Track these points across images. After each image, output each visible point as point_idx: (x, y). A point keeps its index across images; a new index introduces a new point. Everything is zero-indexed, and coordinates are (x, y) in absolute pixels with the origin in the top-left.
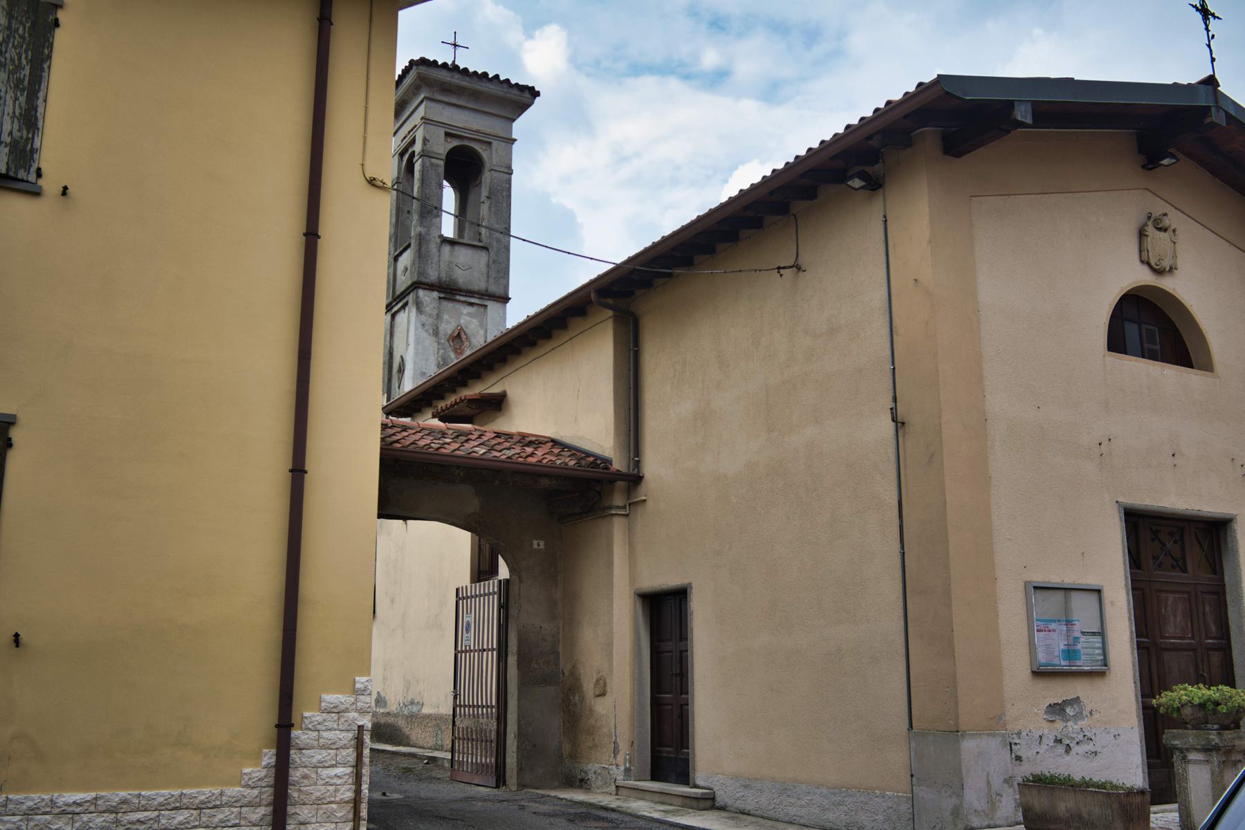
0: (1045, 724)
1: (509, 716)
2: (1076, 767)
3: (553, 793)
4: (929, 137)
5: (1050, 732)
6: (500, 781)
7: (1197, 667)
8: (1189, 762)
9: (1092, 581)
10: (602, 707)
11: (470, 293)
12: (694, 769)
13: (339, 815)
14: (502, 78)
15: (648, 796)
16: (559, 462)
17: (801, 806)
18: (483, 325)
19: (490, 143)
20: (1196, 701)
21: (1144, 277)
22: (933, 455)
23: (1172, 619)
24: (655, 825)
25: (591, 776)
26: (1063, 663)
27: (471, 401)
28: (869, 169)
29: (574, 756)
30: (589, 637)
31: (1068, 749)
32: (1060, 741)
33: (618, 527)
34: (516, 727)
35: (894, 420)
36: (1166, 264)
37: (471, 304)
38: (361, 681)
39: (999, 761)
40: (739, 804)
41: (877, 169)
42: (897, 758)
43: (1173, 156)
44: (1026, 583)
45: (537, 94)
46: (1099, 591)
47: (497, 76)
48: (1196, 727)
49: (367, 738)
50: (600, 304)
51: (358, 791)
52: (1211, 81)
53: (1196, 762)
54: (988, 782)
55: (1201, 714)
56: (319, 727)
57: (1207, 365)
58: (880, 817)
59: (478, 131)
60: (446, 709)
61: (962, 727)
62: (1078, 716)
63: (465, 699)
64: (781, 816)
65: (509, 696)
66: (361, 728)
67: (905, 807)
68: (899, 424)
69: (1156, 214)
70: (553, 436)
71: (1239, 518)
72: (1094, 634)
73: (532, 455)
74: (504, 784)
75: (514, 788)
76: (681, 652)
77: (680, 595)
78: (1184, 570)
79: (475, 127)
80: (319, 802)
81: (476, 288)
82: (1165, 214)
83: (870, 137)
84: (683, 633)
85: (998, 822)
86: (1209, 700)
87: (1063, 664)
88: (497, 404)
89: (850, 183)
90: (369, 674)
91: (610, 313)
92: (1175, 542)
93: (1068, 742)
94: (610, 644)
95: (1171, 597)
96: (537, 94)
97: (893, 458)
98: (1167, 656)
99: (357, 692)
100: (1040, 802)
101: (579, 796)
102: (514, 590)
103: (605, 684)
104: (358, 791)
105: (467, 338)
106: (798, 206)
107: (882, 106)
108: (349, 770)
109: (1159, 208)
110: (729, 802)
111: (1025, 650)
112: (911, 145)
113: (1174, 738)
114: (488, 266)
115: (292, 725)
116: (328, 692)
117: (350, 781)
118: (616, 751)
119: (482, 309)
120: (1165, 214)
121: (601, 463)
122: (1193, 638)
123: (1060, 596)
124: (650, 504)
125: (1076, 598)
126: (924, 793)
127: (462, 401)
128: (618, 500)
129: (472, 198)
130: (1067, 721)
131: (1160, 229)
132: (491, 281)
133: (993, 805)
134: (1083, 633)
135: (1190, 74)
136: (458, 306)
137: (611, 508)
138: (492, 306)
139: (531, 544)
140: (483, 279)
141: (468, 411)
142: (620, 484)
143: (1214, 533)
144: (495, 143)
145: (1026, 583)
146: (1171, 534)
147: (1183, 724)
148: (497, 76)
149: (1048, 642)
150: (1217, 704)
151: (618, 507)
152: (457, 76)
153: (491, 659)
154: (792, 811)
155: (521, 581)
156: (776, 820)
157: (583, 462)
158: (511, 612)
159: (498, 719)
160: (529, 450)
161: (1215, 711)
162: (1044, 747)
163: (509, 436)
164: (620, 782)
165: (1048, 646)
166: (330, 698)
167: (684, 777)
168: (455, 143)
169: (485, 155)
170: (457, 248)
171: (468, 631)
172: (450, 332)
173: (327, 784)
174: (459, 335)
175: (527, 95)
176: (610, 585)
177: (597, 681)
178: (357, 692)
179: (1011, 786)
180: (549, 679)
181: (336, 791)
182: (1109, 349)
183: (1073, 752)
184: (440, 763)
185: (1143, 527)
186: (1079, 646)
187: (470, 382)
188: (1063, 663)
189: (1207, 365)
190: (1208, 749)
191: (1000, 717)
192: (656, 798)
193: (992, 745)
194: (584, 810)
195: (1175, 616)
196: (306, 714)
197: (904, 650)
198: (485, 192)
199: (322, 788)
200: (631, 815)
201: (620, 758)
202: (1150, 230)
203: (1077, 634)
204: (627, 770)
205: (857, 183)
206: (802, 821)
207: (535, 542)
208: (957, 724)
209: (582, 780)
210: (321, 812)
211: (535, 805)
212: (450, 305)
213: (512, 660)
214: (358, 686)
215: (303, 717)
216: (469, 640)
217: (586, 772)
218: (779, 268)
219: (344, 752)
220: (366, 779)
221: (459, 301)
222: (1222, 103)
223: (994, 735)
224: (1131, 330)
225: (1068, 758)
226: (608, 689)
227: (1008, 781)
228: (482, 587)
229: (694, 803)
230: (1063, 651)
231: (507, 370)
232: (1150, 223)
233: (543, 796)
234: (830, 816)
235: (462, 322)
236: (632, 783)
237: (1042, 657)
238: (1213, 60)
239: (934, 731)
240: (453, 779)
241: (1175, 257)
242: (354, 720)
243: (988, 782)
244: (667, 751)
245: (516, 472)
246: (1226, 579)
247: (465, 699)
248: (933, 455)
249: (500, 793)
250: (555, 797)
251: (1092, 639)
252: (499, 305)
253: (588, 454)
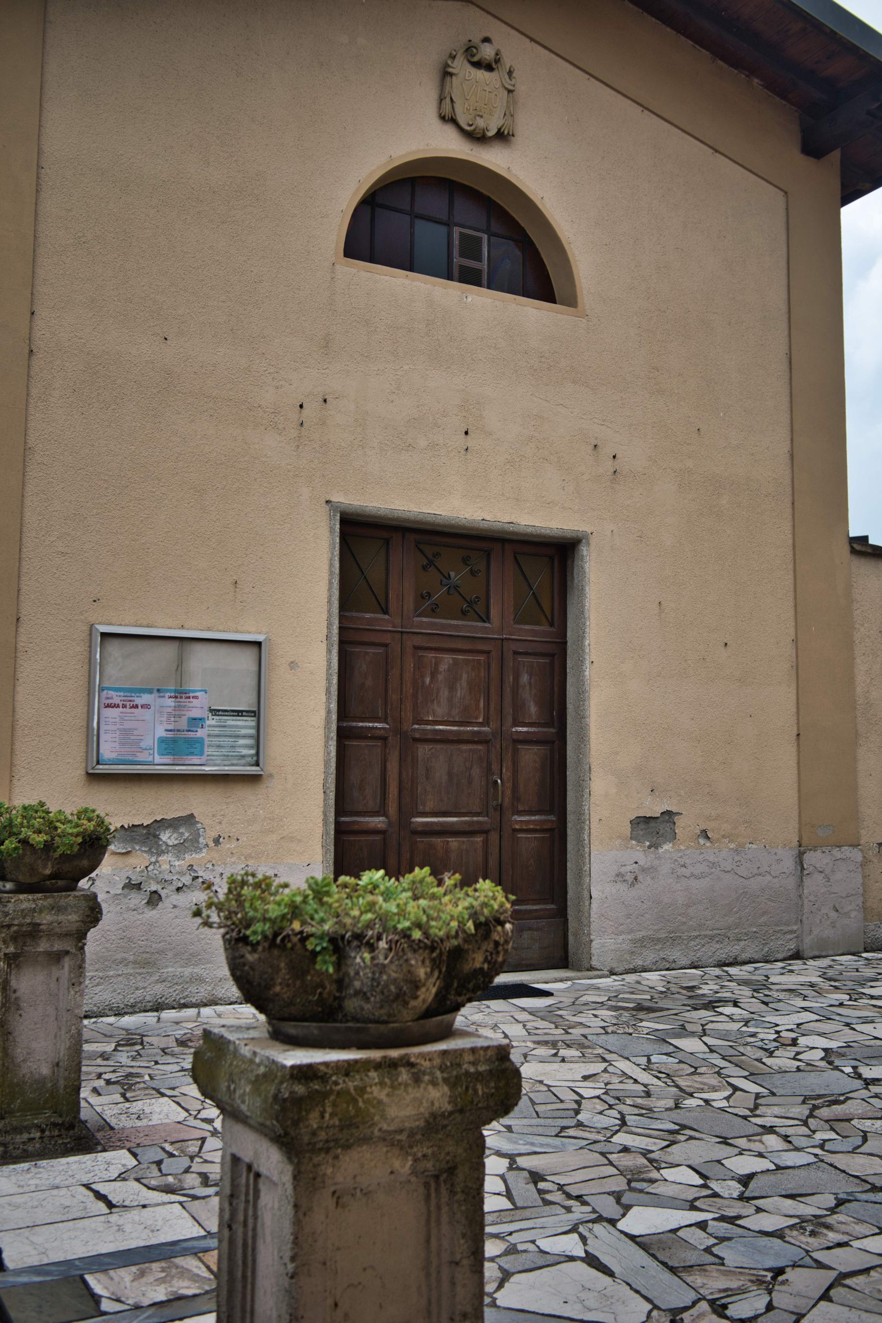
7: (489, 771)
21: (449, 145)
23: (444, 693)
26: (158, 759)
32: (138, 887)
46: (259, 644)
71: (593, 541)
78: (486, 618)
87: (160, 763)
92: (473, 573)
95: (447, 659)
130: (160, 853)
131: (477, 65)
134: (214, 712)
149: (127, 725)
182: (347, 255)
183: (166, 904)
188: (158, 759)
195: (452, 688)
225: (151, 914)
230: (162, 740)
241: (509, 114)
251: (240, 722)
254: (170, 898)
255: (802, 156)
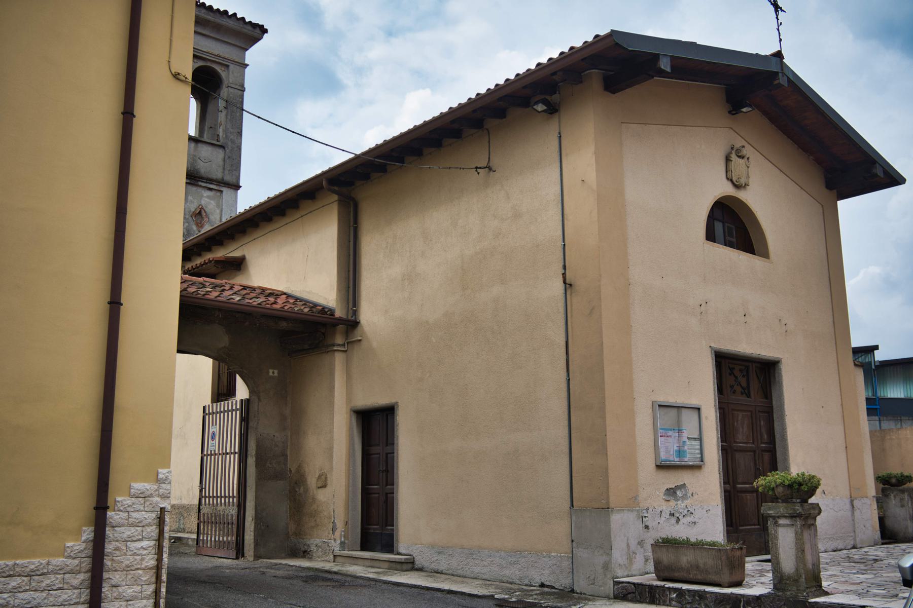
0: (664, 503)
1: (248, 504)
2: (681, 532)
3: (284, 562)
4: (595, 77)
5: (667, 508)
6: (240, 552)
7: (755, 464)
8: (779, 525)
9: (694, 402)
10: (322, 496)
11: (210, 181)
12: (397, 541)
13: (144, 579)
14: (239, 16)
15: (360, 562)
16: (296, 309)
17: (484, 566)
18: (220, 206)
19: (227, 66)
20: (787, 483)
22: (593, 308)
24: (372, 583)
25: (313, 548)
27: (218, 262)
28: (548, 98)
29: (299, 534)
30: (313, 444)
31: (678, 520)
32: (673, 515)
33: (339, 359)
34: (253, 512)
35: (565, 282)
36: (743, 181)
37: (210, 189)
38: (163, 472)
39: (634, 529)
40: (434, 566)
41: (555, 98)
42: (561, 528)
43: (750, 106)
44: (653, 403)
45: (266, 31)
46: (699, 409)
47: (235, 14)
48: (785, 501)
49: (167, 518)
50: (329, 190)
51: (160, 560)
52: (779, 55)
53: (784, 525)
54: (628, 545)
55: (789, 492)
56: (129, 509)
57: (764, 254)
58: (547, 572)
59: (218, 56)
60: (192, 499)
61: (611, 505)
62: (685, 497)
63: (210, 491)
64: (468, 573)
65: (248, 489)
66: (163, 510)
67: (566, 564)
68: (568, 285)
69: (737, 145)
70: (285, 291)
71: (783, 361)
72: (695, 439)
73: (275, 303)
74: (243, 556)
75: (252, 559)
76: (387, 454)
77: (389, 412)
78: (749, 396)
79: (216, 53)
80: (128, 568)
81: (214, 177)
82: (743, 147)
83: (554, 73)
84: (390, 439)
85: (634, 573)
86: (795, 482)
87: (676, 460)
88: (238, 265)
89: (535, 107)
90: (169, 467)
91: (336, 197)
93: (677, 515)
94: (331, 449)
95: (740, 414)
96: (266, 31)
97: (562, 310)
98: (738, 455)
99: (158, 481)
100: (667, 557)
101: (305, 563)
102: (254, 407)
103: (326, 478)
104: (160, 560)
105: (207, 215)
106: (491, 123)
107: (566, 50)
108: (154, 542)
109: (739, 142)
110: (426, 564)
111: (652, 449)
112: (581, 82)
113: (770, 509)
114: (224, 160)
115: (108, 508)
116: (136, 481)
117: (153, 552)
118: (334, 529)
119: (218, 194)
120: (743, 147)
121: (326, 311)
122: (753, 443)
123: (675, 411)
124: (364, 343)
125: (685, 414)
126: (582, 554)
127: (210, 261)
128: (339, 340)
129: (211, 108)
130: (678, 500)
131: (739, 157)
132: (226, 172)
133: (630, 560)
135: (767, 49)
136: (200, 190)
137: (334, 345)
138: (227, 192)
139: (268, 372)
140: (220, 170)
141: (213, 270)
142: (341, 328)
143: (767, 370)
144: (232, 67)
145: (653, 403)
146: (741, 370)
147: (775, 499)
148: (235, 14)
150: (800, 484)
151: (339, 345)
152: (204, 11)
153: (233, 462)
154: (477, 570)
155: (259, 400)
156: (464, 577)
157: (314, 310)
158: (251, 424)
159: (239, 506)
160: (272, 299)
161: (799, 490)
162: (663, 519)
163: (253, 289)
164: (337, 553)
165: (667, 448)
166: (138, 486)
167: (389, 545)
168: (200, 63)
169: (223, 74)
170: (200, 145)
171: (213, 439)
172: (193, 210)
173: (135, 554)
174: (200, 213)
175: (258, 31)
176: (332, 404)
177: (320, 476)
178: (158, 481)
179: (642, 547)
180: (277, 476)
181: (142, 560)
183: (681, 523)
184: (184, 541)
185: (728, 366)
186: (686, 448)
187: (214, 248)
189: (764, 254)
190: (792, 517)
191: (635, 498)
192: (368, 563)
193: (630, 517)
194: (311, 573)
196: (119, 499)
197: (567, 450)
198: (221, 104)
199: (131, 558)
200: (350, 576)
201: (337, 534)
202: (733, 157)
203: (685, 439)
204: (343, 544)
205: (540, 107)
206: (484, 577)
207: (271, 371)
208: (608, 502)
209: (305, 552)
210: (129, 577)
211: (273, 571)
212: (194, 189)
213: (251, 461)
214: (160, 476)
215: (115, 501)
216: (213, 446)
217: (309, 546)
218: (477, 168)
219: (149, 529)
220: (166, 549)
221: (201, 186)
222: (786, 71)
223: (632, 511)
224: (719, 227)
225: (678, 527)
226: (329, 482)
227: (641, 543)
228: (222, 406)
229: (398, 566)
231: (246, 240)
232: (733, 152)
233: (276, 564)
234: (507, 572)
235: (203, 202)
236: (346, 553)
237: (663, 455)
238: (780, 40)
239: (589, 510)
240: (197, 554)
241: (748, 177)
242: (157, 503)
243: (628, 545)
244: (374, 528)
245: (264, 316)
246: (774, 403)
247: (210, 491)
248: (593, 308)
249: (241, 562)
250: (286, 564)
252: (232, 191)
253: (315, 305)
254: (683, 520)
255: (825, 191)
